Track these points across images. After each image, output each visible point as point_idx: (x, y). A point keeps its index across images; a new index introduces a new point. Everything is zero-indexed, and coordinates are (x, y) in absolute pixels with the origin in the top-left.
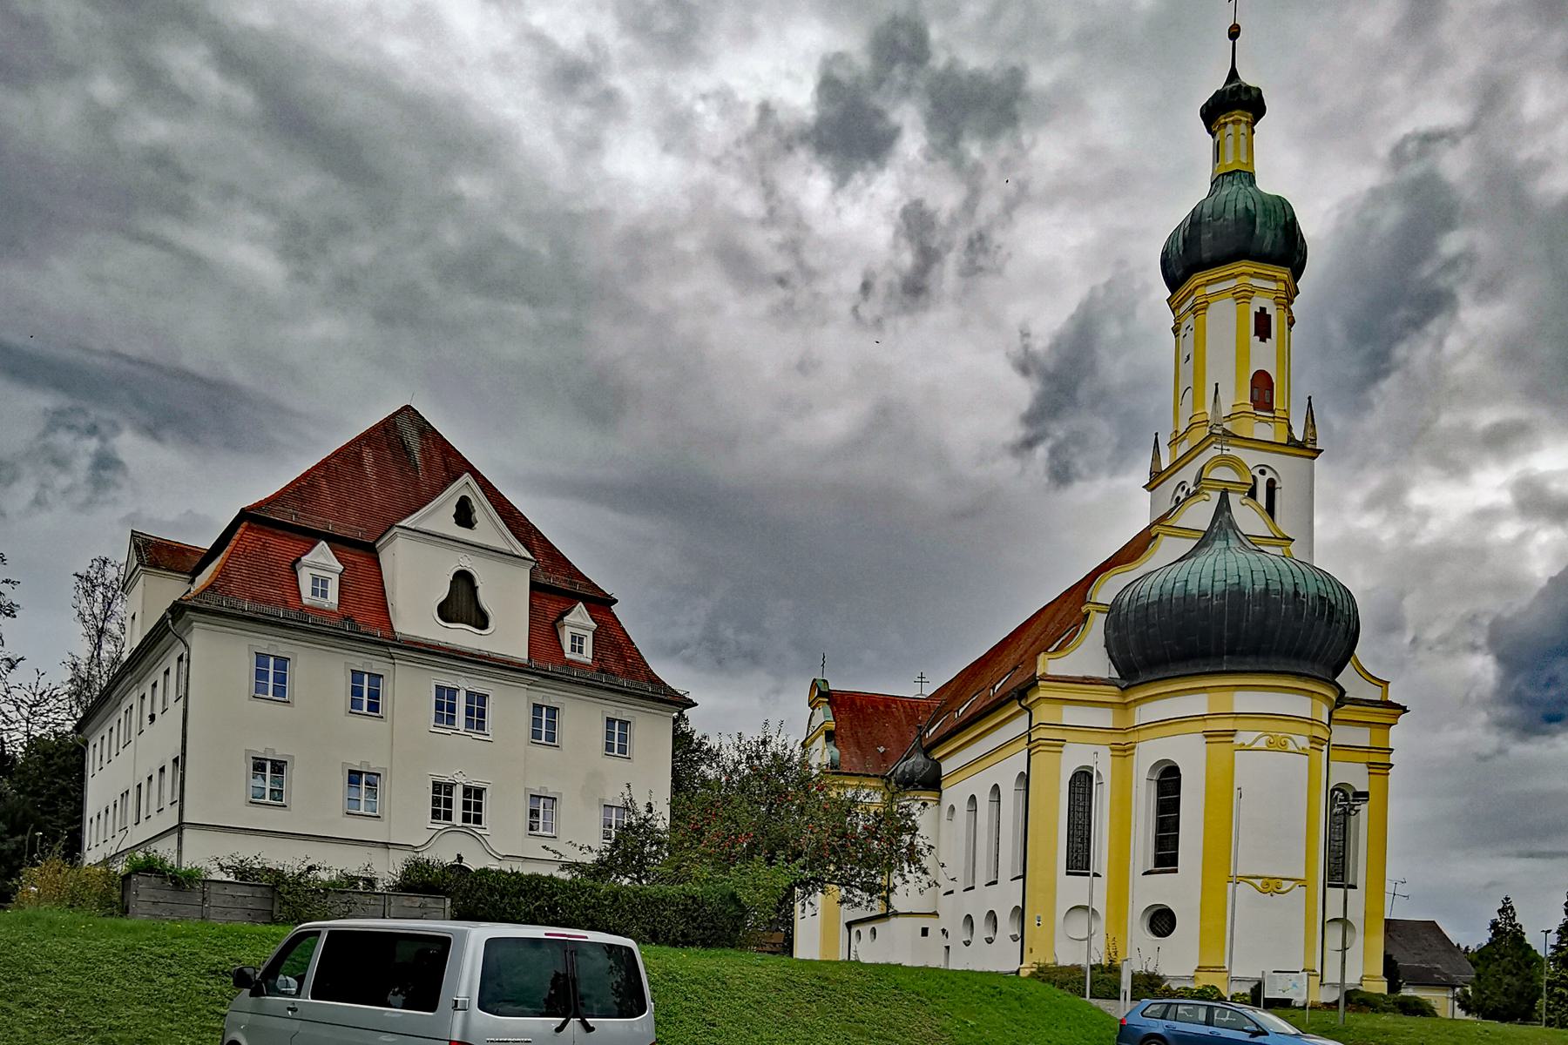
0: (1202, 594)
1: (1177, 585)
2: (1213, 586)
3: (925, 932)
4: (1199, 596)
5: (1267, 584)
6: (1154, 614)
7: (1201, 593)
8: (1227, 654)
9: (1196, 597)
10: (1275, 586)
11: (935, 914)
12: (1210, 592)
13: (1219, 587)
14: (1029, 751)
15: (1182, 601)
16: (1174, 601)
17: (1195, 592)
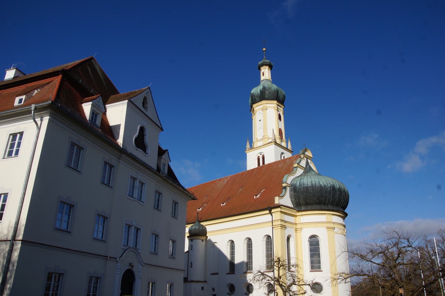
0: (325, 186)
1: (317, 182)
2: (327, 185)
3: (203, 288)
4: (324, 187)
5: (339, 186)
6: (311, 189)
7: (325, 186)
8: (330, 205)
9: (323, 187)
10: (341, 187)
11: (205, 282)
12: (327, 186)
13: (329, 185)
14: (273, 228)
15: (319, 187)
16: (317, 187)
17: (323, 185)
